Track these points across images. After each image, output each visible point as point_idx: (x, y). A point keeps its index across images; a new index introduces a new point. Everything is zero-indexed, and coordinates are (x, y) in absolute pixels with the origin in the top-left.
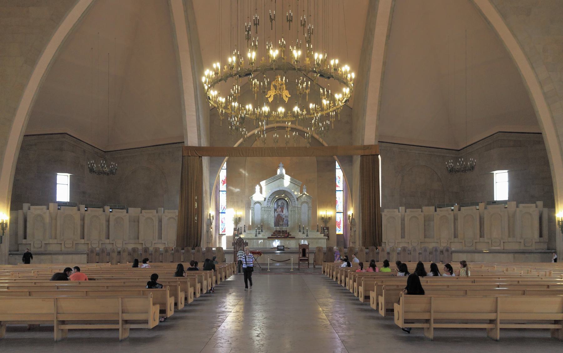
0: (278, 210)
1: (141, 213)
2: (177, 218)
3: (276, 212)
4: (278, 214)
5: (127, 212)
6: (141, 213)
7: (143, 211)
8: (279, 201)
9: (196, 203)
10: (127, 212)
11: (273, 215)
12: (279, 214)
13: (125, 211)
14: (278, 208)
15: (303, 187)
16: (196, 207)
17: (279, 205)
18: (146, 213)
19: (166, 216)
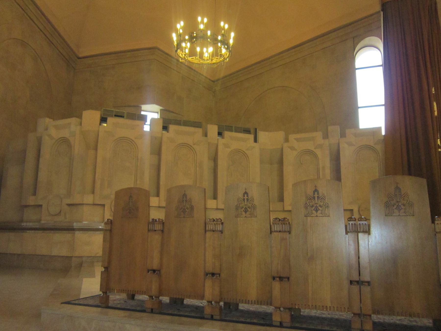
1: (287, 140)
2: (379, 148)
5: (256, 141)
6: (287, 140)
7: (292, 137)
9: (435, 104)
10: (256, 141)
13: (251, 137)
16: (436, 113)
18: (297, 140)
19: (350, 144)
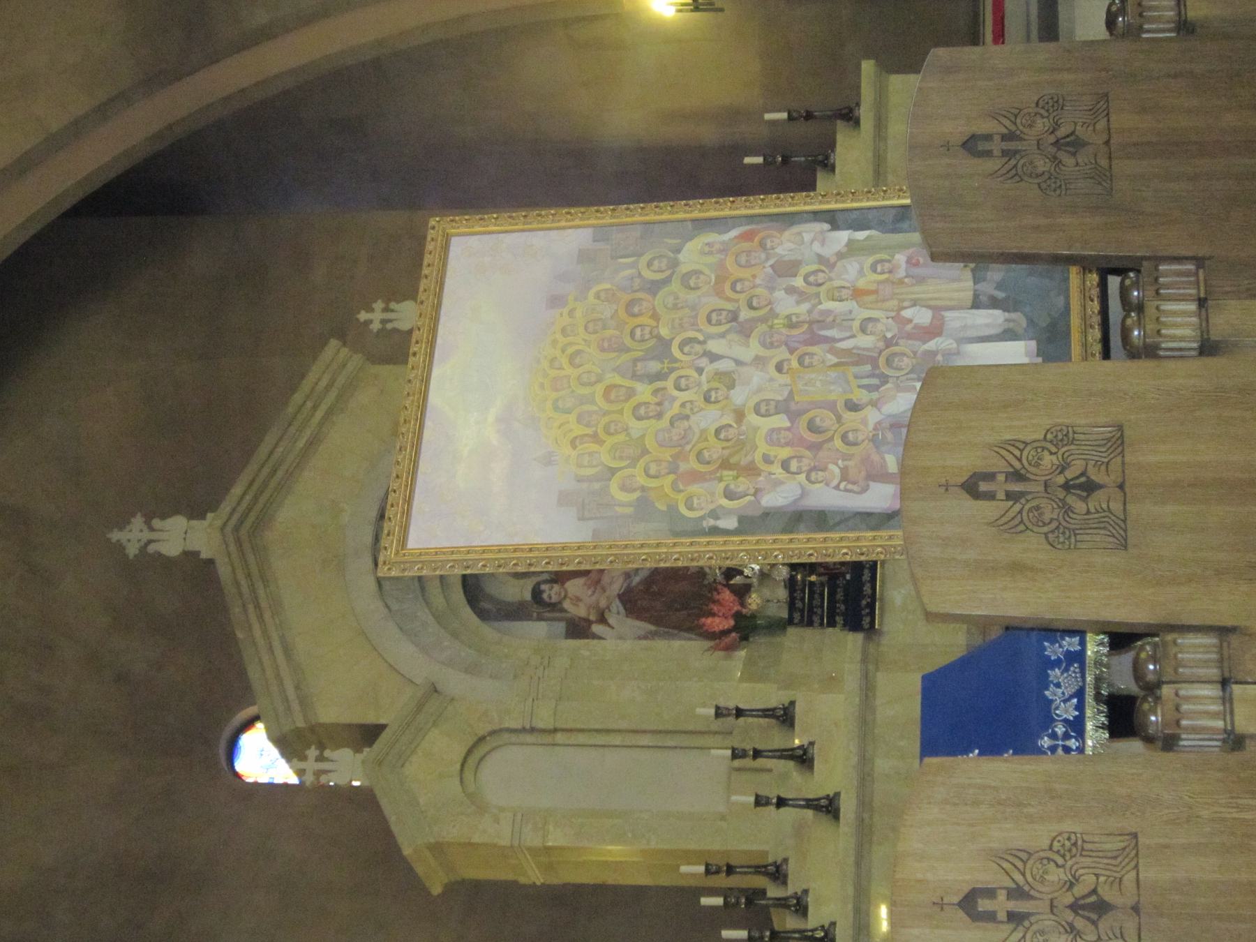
0: (581, 611)
3: (597, 628)
4: (617, 605)
8: (491, 599)
11: (627, 645)
12: (620, 597)
14: (555, 607)
15: (376, 326)
17: (528, 596)
